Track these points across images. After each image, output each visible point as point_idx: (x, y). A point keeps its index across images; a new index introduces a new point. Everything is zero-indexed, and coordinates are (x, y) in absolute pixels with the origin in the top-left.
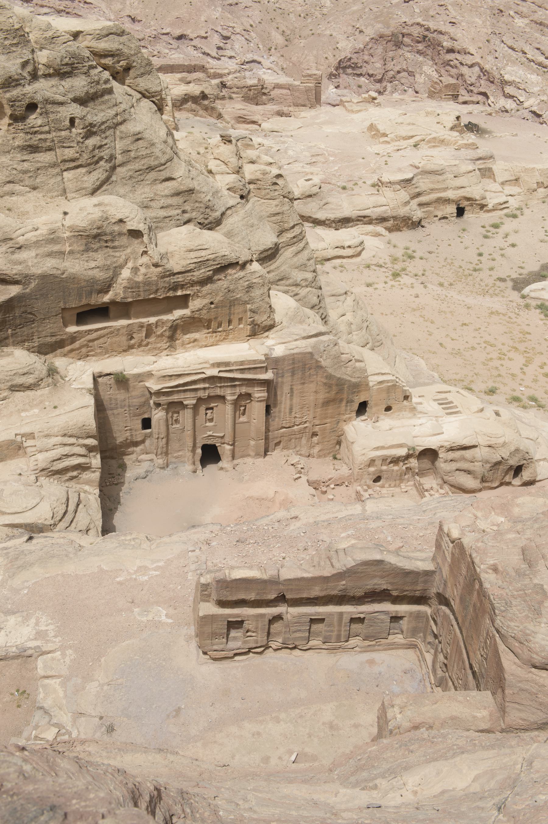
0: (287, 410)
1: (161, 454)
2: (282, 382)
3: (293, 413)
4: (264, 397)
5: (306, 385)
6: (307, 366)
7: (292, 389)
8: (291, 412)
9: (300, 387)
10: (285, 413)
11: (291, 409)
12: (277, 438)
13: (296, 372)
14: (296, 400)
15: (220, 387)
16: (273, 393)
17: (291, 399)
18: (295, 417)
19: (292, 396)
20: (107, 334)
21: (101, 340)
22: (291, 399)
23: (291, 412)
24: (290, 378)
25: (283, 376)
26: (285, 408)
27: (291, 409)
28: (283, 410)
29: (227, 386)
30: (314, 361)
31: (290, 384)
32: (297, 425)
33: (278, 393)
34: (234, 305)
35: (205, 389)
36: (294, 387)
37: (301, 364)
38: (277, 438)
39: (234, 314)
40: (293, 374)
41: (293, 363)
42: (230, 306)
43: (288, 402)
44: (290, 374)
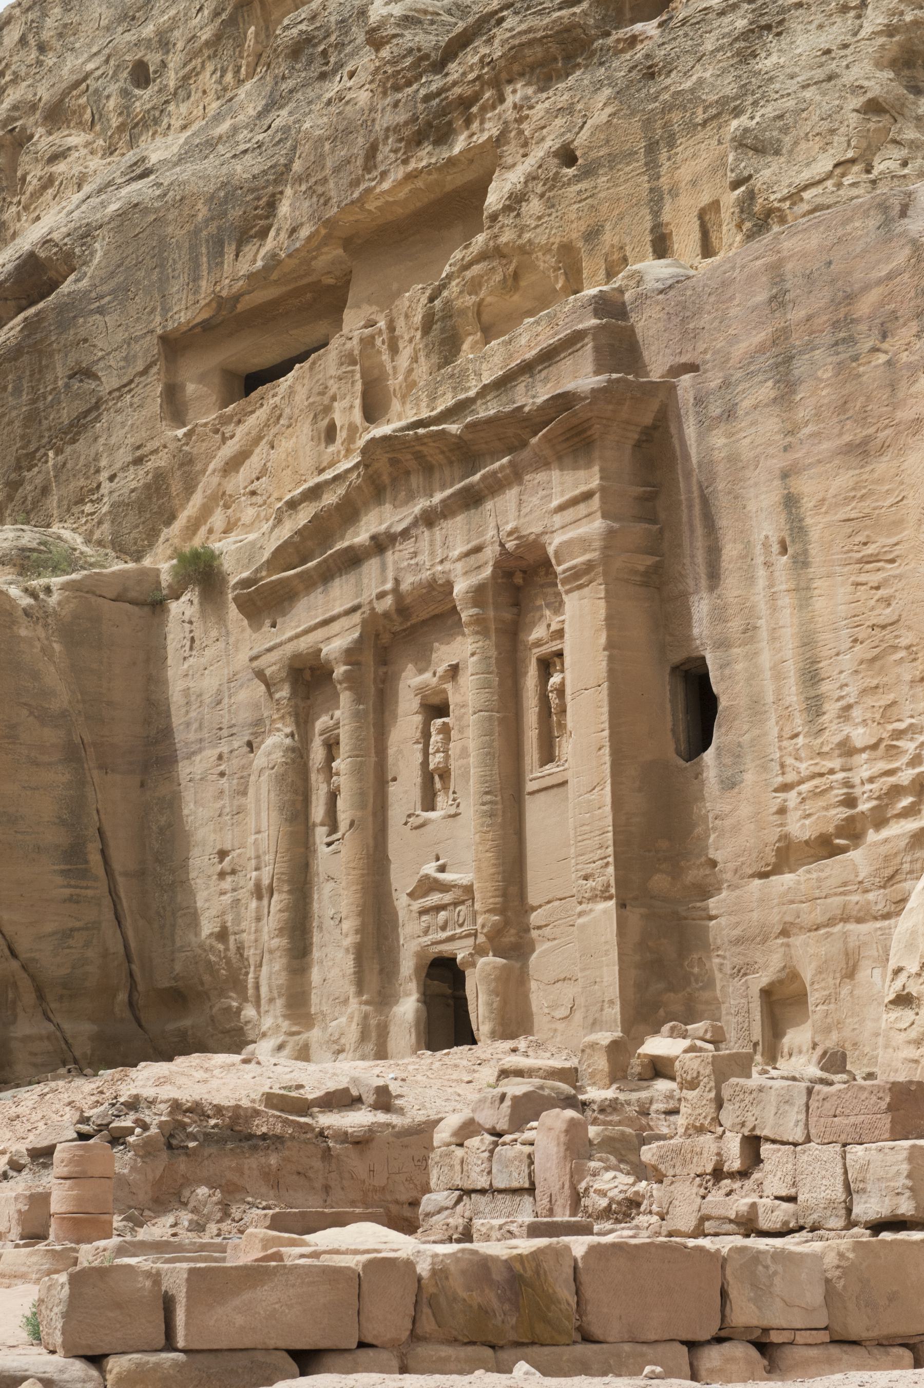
0: (793, 695)
1: (271, 1000)
2: (733, 459)
3: (832, 708)
4: (583, 543)
5: (882, 466)
6: (864, 306)
7: (790, 502)
8: (814, 707)
9: (844, 480)
10: (786, 717)
11: (811, 676)
12: (762, 937)
13: (800, 367)
14: (833, 598)
15: (429, 519)
16: (700, 557)
17: (803, 592)
18: (847, 749)
19: (801, 562)
20: (267, 425)
21: (254, 462)
22: (803, 592)
23: (814, 707)
24: (771, 424)
25: (730, 414)
26: (778, 676)
27: (811, 676)
28: (770, 698)
29: (446, 511)
30: (902, 256)
31: (778, 463)
32: (880, 820)
33: (730, 551)
34: (671, 143)
35: (381, 544)
36: (808, 487)
37: (820, 299)
38: (762, 937)
39: (674, 192)
40: (787, 388)
41: (778, 301)
42: (652, 148)
43: (788, 617)
44: (766, 391)
